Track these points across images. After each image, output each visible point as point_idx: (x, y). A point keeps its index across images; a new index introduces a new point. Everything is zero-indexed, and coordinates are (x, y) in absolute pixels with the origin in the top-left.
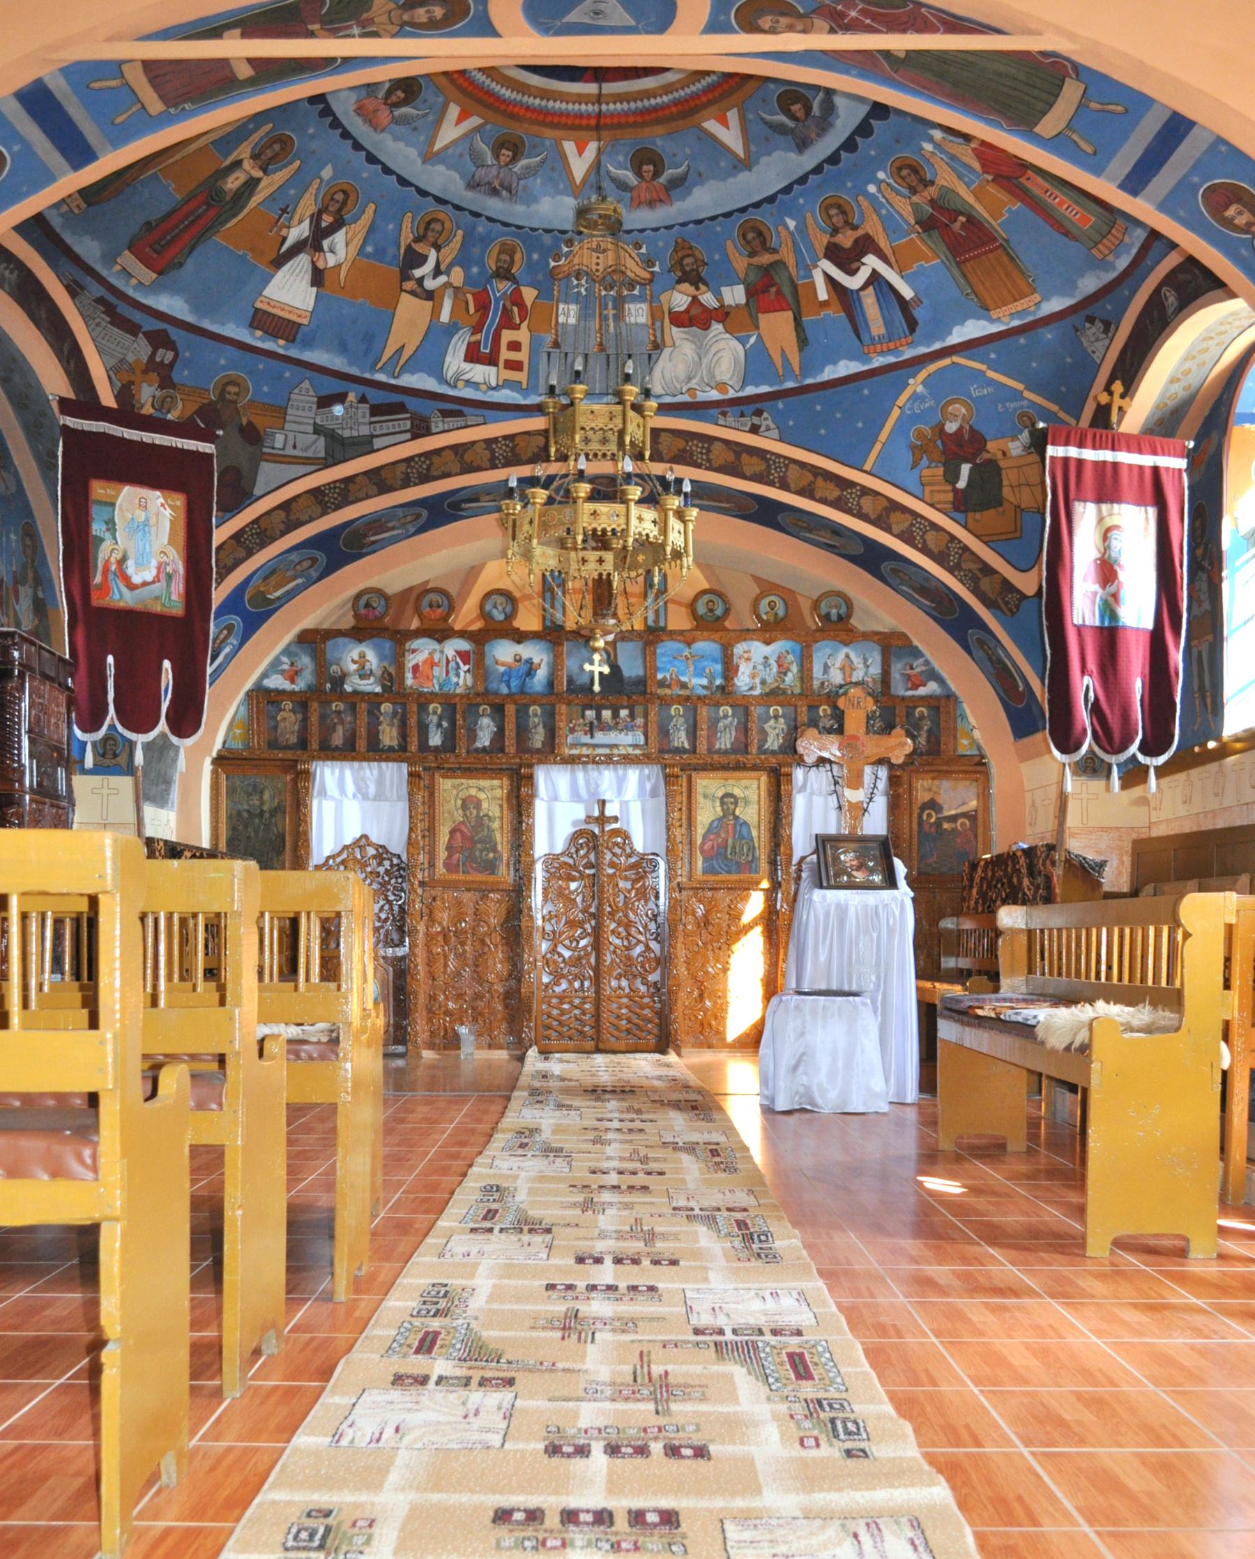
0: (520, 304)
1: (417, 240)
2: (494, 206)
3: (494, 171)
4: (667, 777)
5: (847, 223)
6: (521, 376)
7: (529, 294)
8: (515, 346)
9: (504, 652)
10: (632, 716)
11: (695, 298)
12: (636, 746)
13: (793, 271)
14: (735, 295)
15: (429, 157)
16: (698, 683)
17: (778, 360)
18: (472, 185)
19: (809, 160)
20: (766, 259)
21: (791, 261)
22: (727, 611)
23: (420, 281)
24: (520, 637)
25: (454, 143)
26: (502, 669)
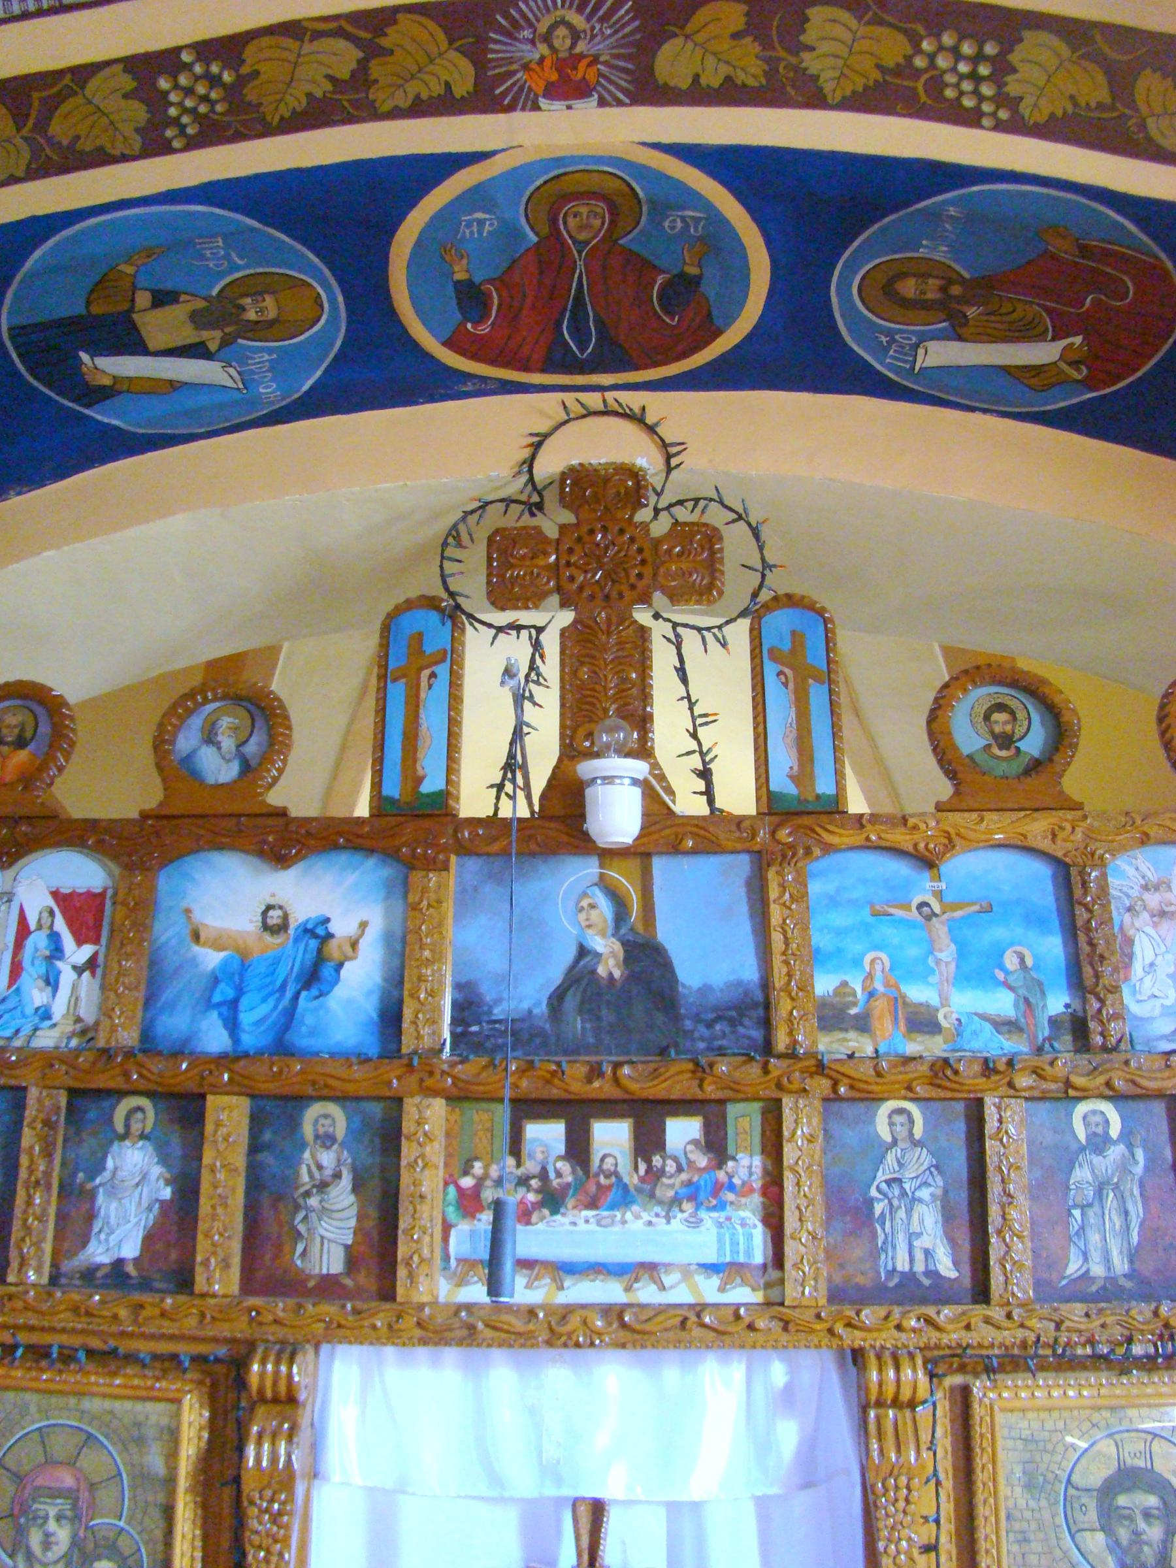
4: (864, 1406)
9: (224, 899)
10: (716, 1144)
12: (728, 1271)
16: (974, 1010)
22: (1062, 734)
24: (285, 841)
26: (211, 959)
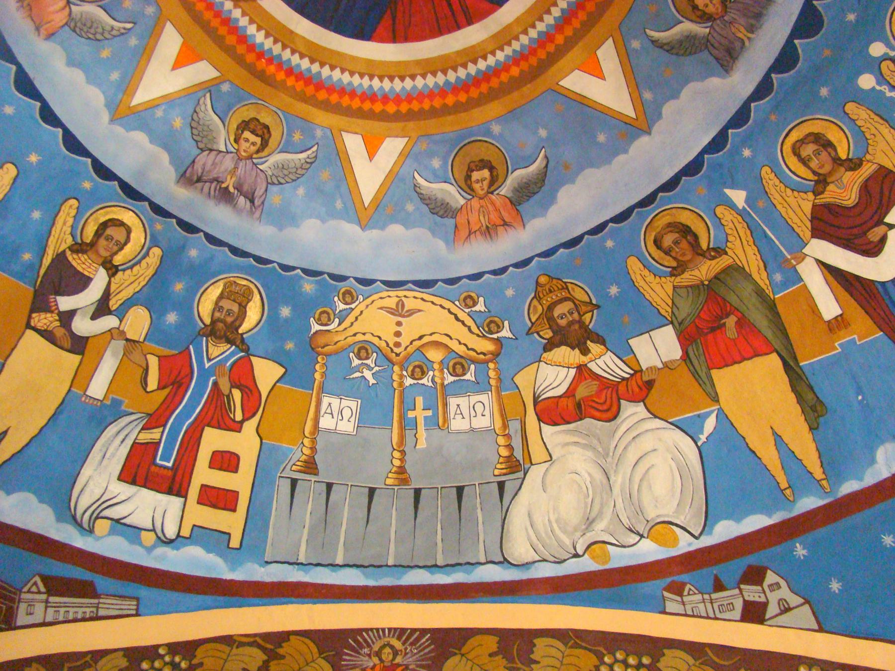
0: (249, 389)
1: (79, 248)
2: (220, 218)
3: (228, 163)
5: (837, 161)
6: (231, 522)
7: (266, 373)
8: (226, 461)
11: (581, 369)
13: (761, 278)
14: (659, 347)
15: (121, 113)
17: (770, 456)
18: (189, 178)
19: (743, 80)
20: (705, 270)
21: (752, 263)
23: (67, 317)
25: (169, 100)
